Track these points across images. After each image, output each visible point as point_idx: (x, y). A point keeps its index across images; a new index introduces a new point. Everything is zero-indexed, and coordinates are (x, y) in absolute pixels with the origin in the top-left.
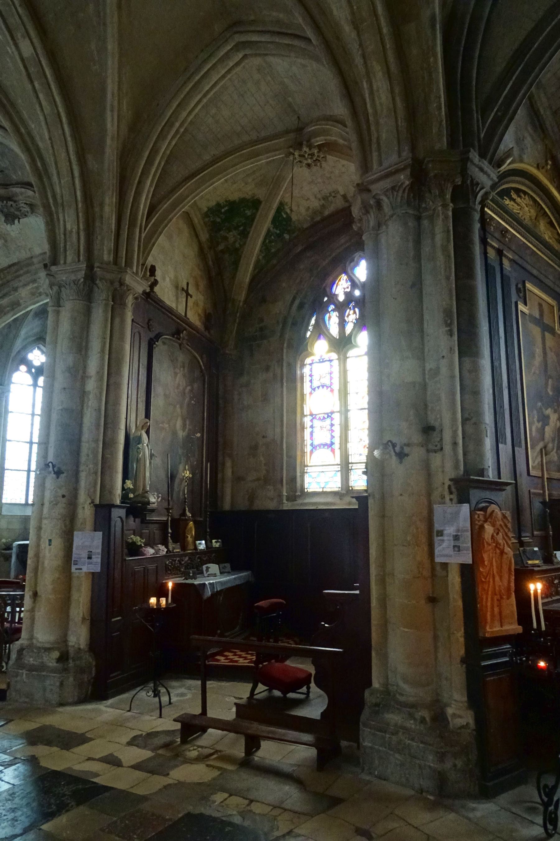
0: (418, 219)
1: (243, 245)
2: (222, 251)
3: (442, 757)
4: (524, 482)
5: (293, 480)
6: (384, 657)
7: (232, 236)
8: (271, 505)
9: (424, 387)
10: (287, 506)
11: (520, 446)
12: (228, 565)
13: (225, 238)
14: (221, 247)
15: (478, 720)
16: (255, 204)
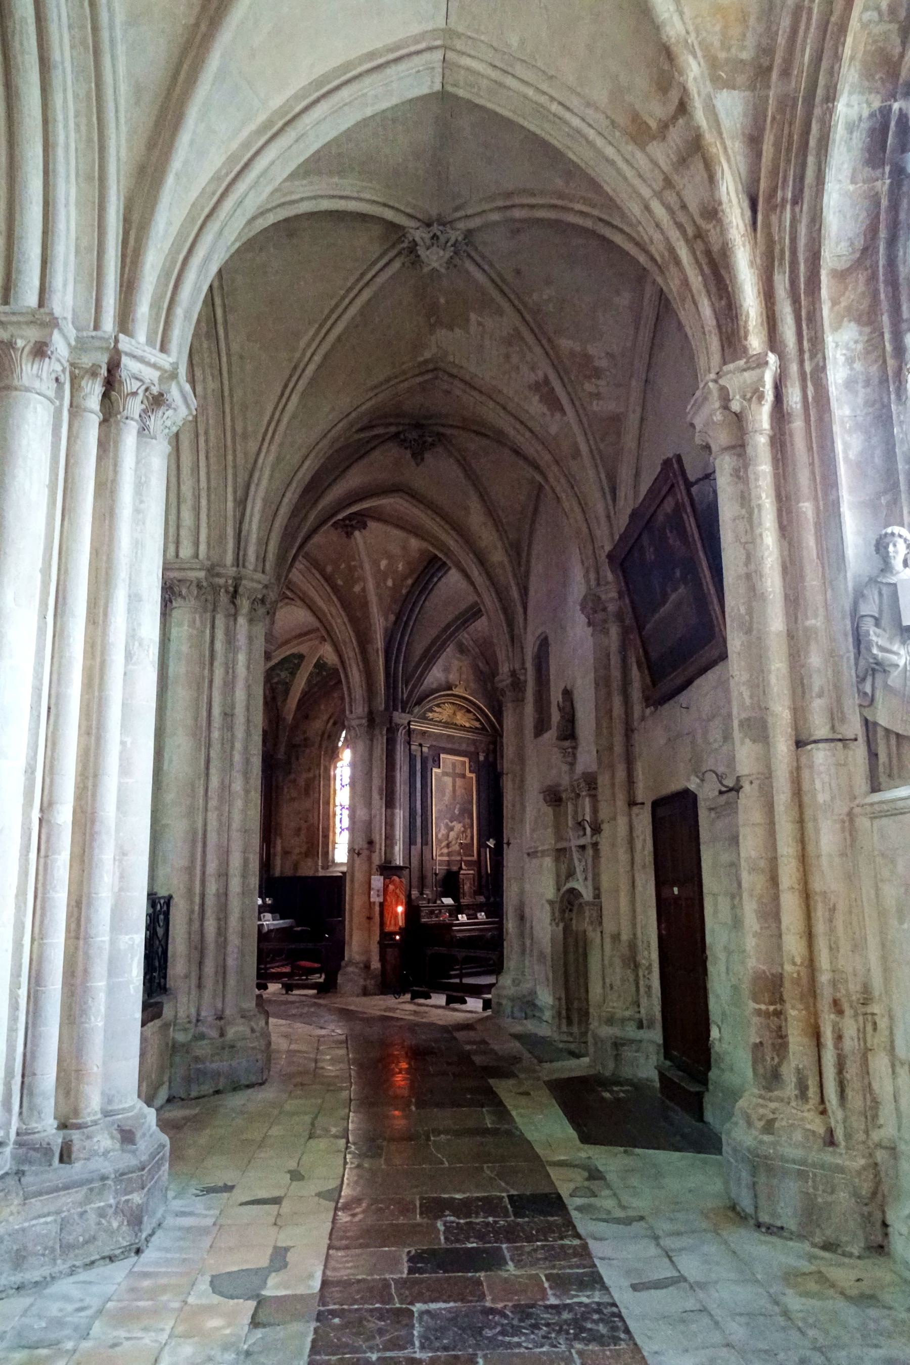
0: (372, 740)
1: (292, 681)
2: (277, 683)
3: (365, 980)
4: (428, 865)
5: (326, 854)
6: (350, 945)
7: (284, 674)
8: (311, 873)
9: (370, 822)
10: (321, 873)
11: (427, 844)
12: (278, 916)
13: (278, 675)
14: (275, 680)
15: (383, 966)
16: (301, 657)
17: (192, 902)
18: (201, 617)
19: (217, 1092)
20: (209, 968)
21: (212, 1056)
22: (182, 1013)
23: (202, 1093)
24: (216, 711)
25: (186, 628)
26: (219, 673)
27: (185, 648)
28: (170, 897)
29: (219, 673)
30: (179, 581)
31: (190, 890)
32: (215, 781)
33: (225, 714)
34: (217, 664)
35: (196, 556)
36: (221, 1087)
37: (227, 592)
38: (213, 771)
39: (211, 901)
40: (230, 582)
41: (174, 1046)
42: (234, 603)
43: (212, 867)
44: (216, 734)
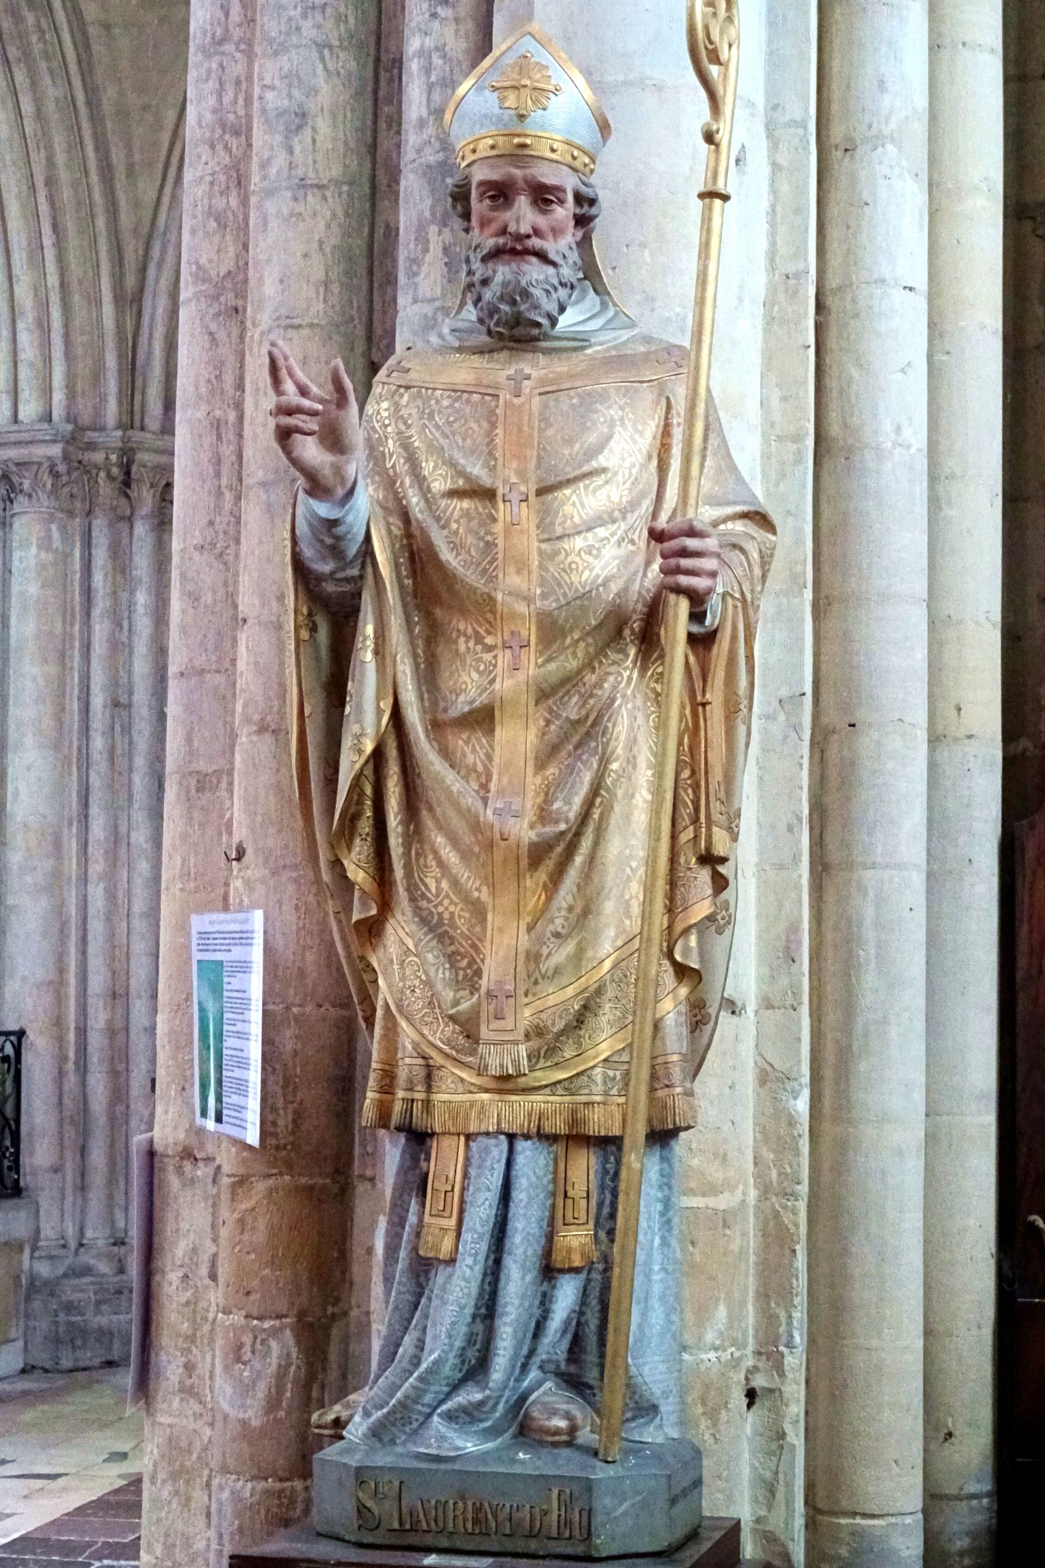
17: (61, 1039)
18: (63, 529)
19: (110, 1364)
20: (98, 1157)
21: (98, 1303)
22: (48, 1231)
23: (81, 1364)
24: (98, 701)
25: (34, 550)
26: (100, 630)
27: (33, 589)
28: (21, 1034)
29: (100, 630)
30: (18, 464)
31: (58, 1022)
32: (98, 829)
33: (116, 704)
34: (96, 612)
35: (48, 418)
36: (115, 1356)
37: (110, 477)
38: (94, 810)
39: (96, 1041)
40: (114, 457)
41: (32, 1285)
42: (127, 496)
43: (98, 981)
44: (98, 743)
